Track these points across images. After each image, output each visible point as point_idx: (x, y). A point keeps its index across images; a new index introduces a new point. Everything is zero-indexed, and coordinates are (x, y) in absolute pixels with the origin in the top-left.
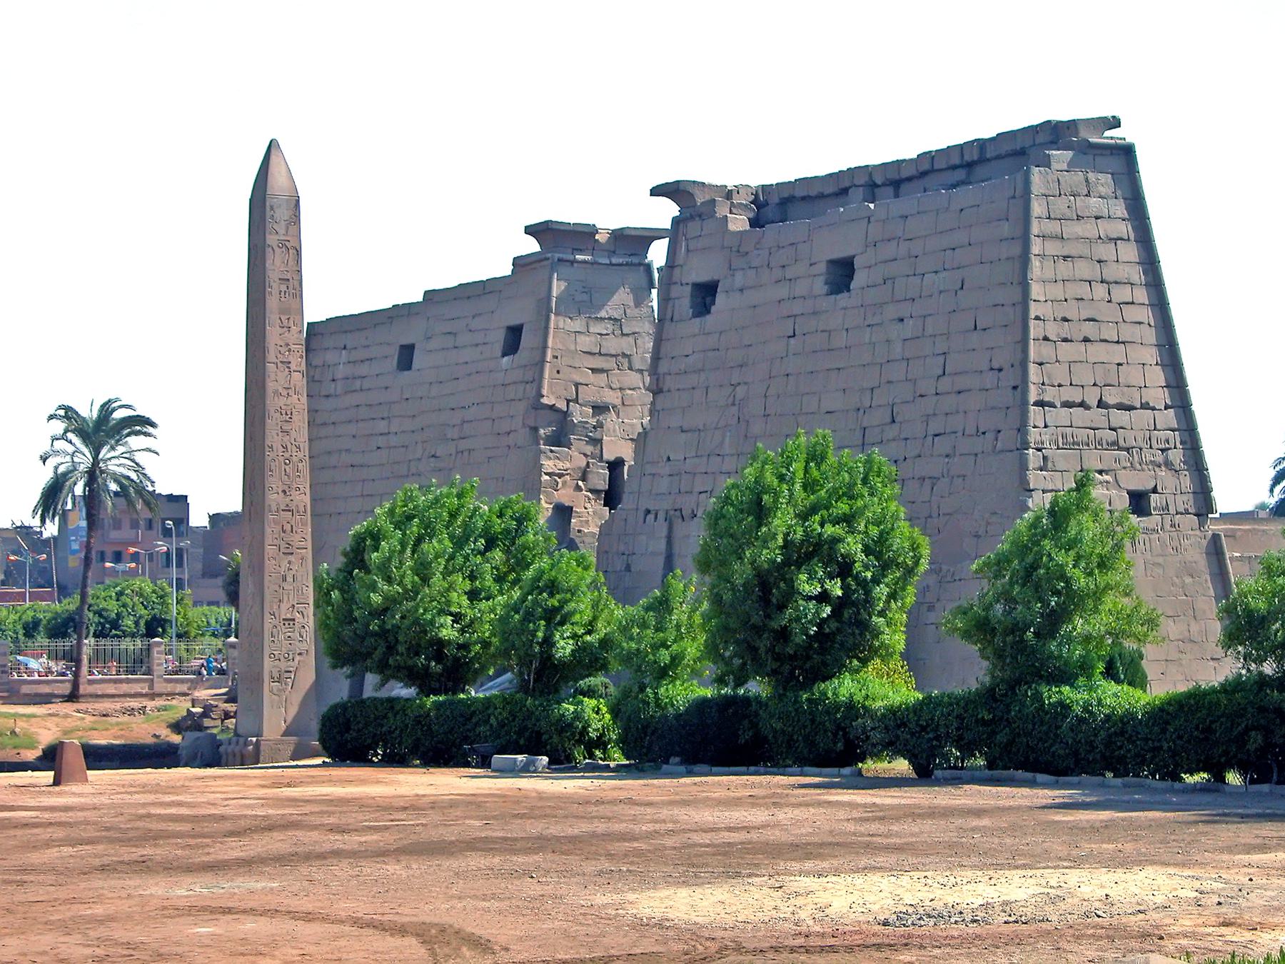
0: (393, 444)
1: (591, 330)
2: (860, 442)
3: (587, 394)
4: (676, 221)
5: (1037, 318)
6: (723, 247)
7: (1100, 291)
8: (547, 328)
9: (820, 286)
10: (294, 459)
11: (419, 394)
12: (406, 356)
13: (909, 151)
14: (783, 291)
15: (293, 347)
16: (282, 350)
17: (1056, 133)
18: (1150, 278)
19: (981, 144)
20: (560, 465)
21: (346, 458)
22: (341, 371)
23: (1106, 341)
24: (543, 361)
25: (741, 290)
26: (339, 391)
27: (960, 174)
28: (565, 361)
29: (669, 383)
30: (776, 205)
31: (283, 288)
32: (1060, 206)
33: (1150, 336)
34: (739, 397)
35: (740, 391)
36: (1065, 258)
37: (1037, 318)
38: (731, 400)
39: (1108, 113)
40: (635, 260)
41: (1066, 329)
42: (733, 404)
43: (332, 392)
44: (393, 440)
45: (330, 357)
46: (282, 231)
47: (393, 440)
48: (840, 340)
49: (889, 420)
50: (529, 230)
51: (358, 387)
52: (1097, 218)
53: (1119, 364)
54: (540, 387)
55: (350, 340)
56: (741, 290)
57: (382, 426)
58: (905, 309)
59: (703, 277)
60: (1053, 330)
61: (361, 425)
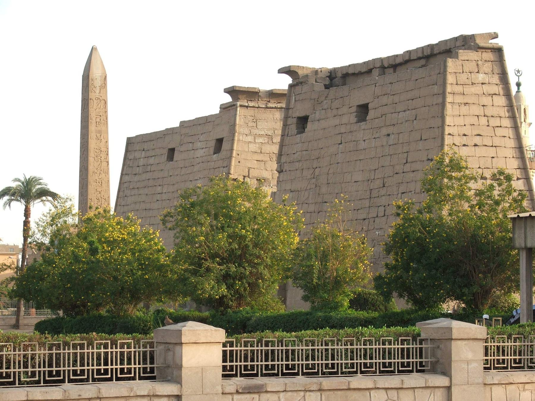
0: (164, 198)
1: (256, 141)
2: (368, 197)
3: (253, 173)
4: (291, 86)
5: (449, 134)
6: (311, 99)
7: (483, 121)
8: (233, 140)
9: (353, 119)
11: (176, 173)
13: (400, 51)
14: (337, 121)
16: (97, 151)
17: (466, 42)
18: (510, 114)
19: (431, 47)
21: (143, 206)
22: (142, 162)
23: (486, 146)
25: (319, 120)
27: (423, 62)
28: (243, 156)
29: (286, 167)
30: (338, 79)
32: (463, 78)
33: (512, 143)
34: (316, 174)
35: (317, 171)
36: (466, 104)
37: (449, 134)
38: (312, 176)
39: (492, 31)
41: (464, 140)
42: (314, 178)
43: (137, 172)
44: (164, 197)
45: (137, 155)
46: (98, 91)
47: (164, 197)
48: (362, 145)
49: (382, 185)
51: (149, 170)
52: (482, 84)
53: (493, 157)
56: (319, 120)
57: (159, 189)
58: (390, 130)
59: (302, 114)
60: (458, 140)
61: (150, 189)
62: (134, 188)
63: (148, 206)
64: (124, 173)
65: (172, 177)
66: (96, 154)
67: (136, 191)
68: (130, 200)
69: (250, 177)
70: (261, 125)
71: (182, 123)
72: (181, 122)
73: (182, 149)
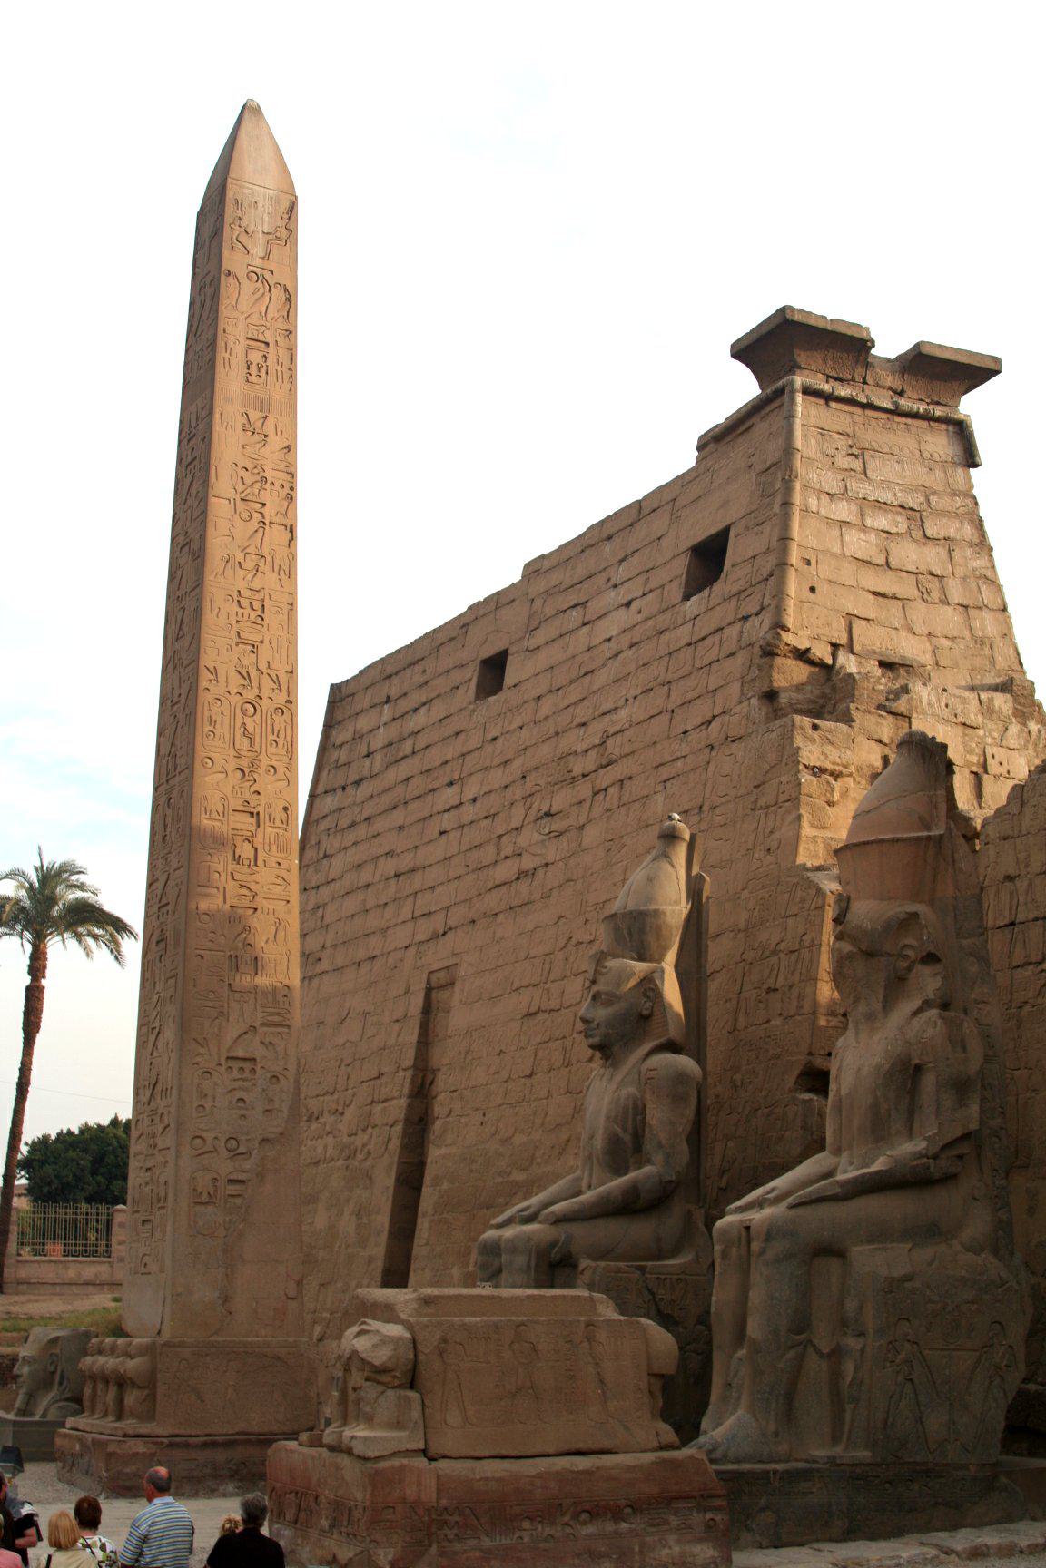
1: (869, 522)
8: (787, 504)
10: (265, 703)
11: (515, 725)
12: (494, 670)
15: (269, 474)
20: (834, 754)
21: (389, 866)
24: (783, 564)
26: (378, 766)
28: (824, 570)
31: (256, 357)
40: (939, 411)
43: (366, 773)
44: (469, 812)
45: (364, 723)
46: (259, 250)
47: (469, 812)
50: (746, 351)
54: (779, 609)
55: (394, 688)
57: (450, 795)
61: (413, 806)
62: (353, 825)
63: (405, 863)
64: (320, 789)
65: (500, 741)
66: (240, 487)
67: (362, 831)
68: (337, 865)
69: (857, 648)
70: (880, 469)
71: (534, 569)
72: (527, 566)
73: (533, 643)
